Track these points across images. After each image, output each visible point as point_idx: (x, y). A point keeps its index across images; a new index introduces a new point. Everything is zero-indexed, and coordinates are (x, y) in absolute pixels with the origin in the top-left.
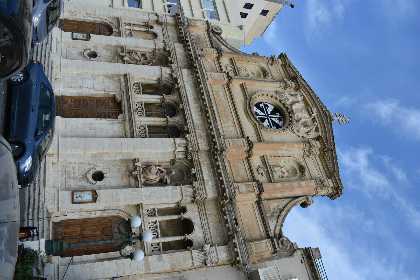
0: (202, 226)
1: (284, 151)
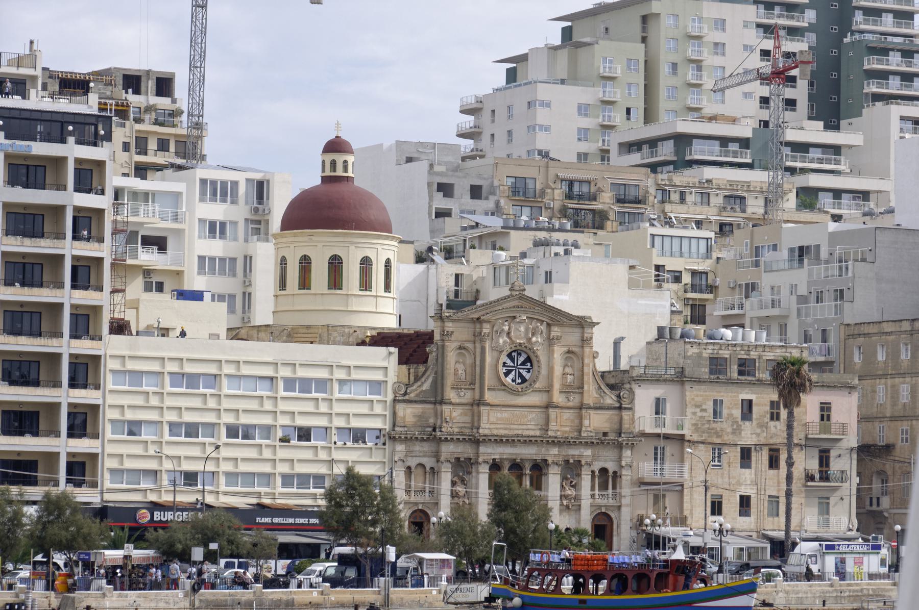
0: (606, 461)
1: (558, 370)
